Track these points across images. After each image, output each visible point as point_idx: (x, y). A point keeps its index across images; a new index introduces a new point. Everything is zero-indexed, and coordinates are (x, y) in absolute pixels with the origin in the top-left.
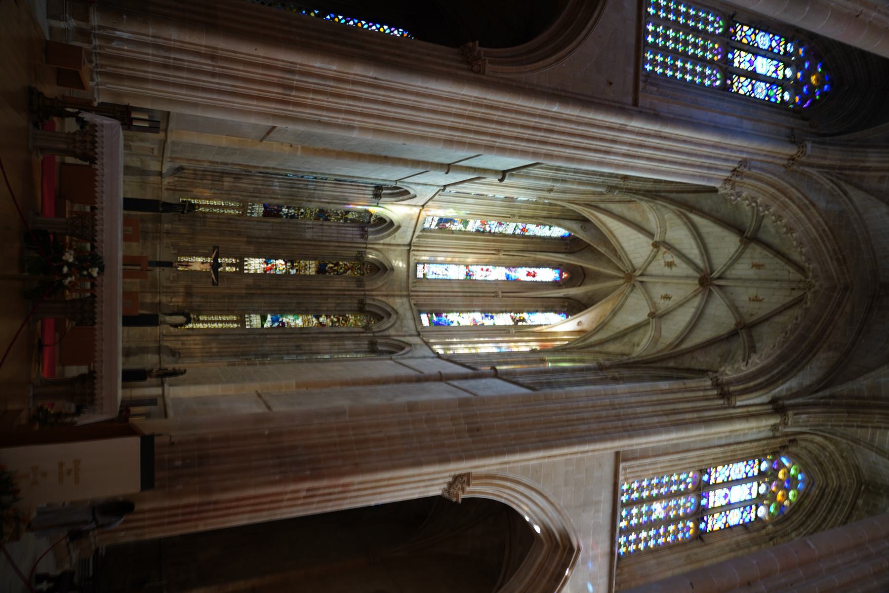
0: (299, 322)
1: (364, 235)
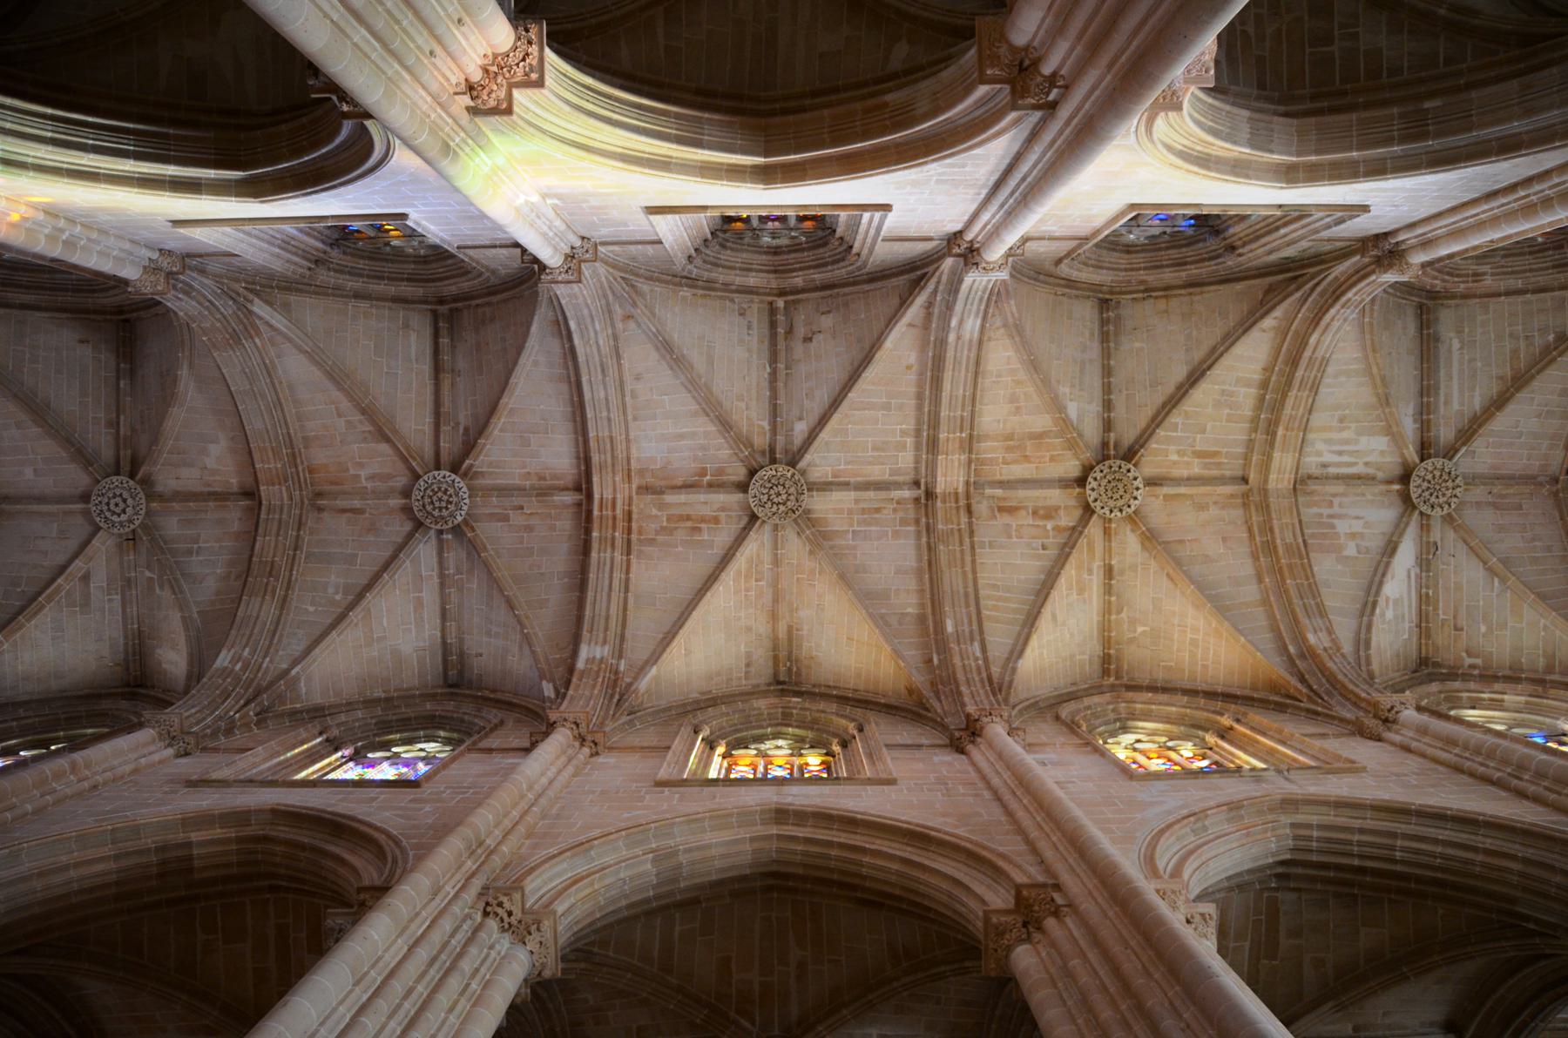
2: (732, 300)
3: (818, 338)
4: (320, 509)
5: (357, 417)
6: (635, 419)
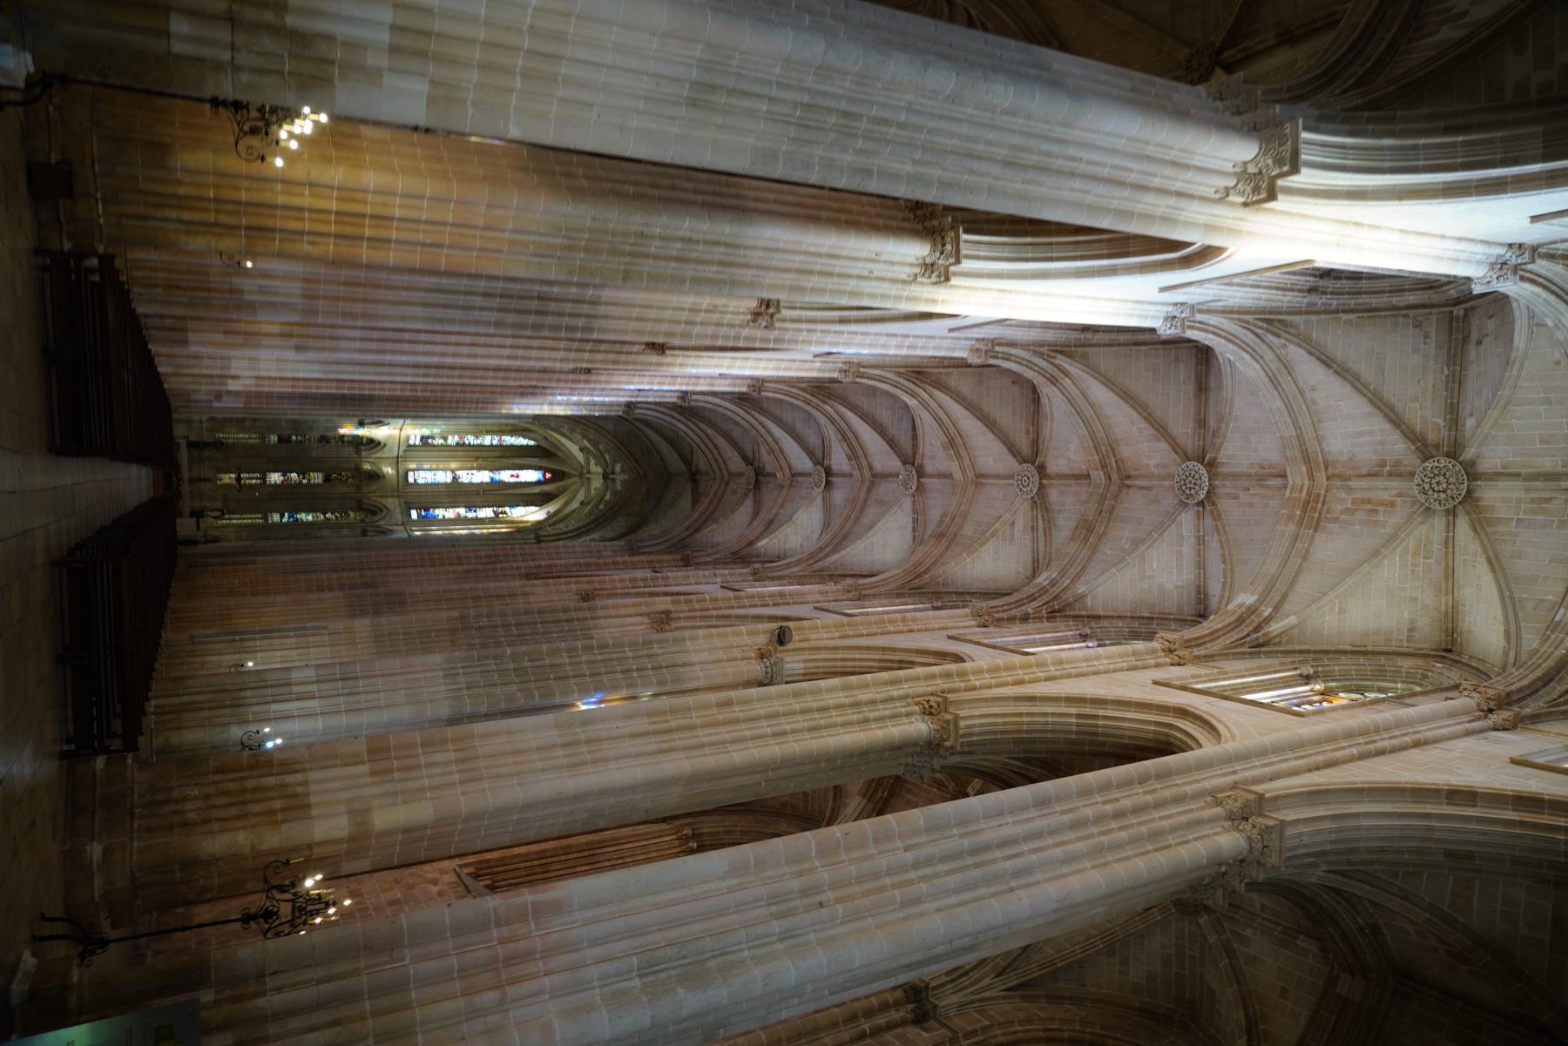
0: (310, 518)
1: (358, 452)
2: (1406, 316)
3: (1486, 340)
4: (1129, 487)
5: (1144, 425)
6: (1320, 421)
